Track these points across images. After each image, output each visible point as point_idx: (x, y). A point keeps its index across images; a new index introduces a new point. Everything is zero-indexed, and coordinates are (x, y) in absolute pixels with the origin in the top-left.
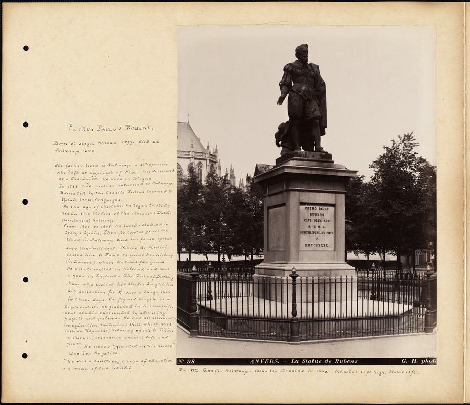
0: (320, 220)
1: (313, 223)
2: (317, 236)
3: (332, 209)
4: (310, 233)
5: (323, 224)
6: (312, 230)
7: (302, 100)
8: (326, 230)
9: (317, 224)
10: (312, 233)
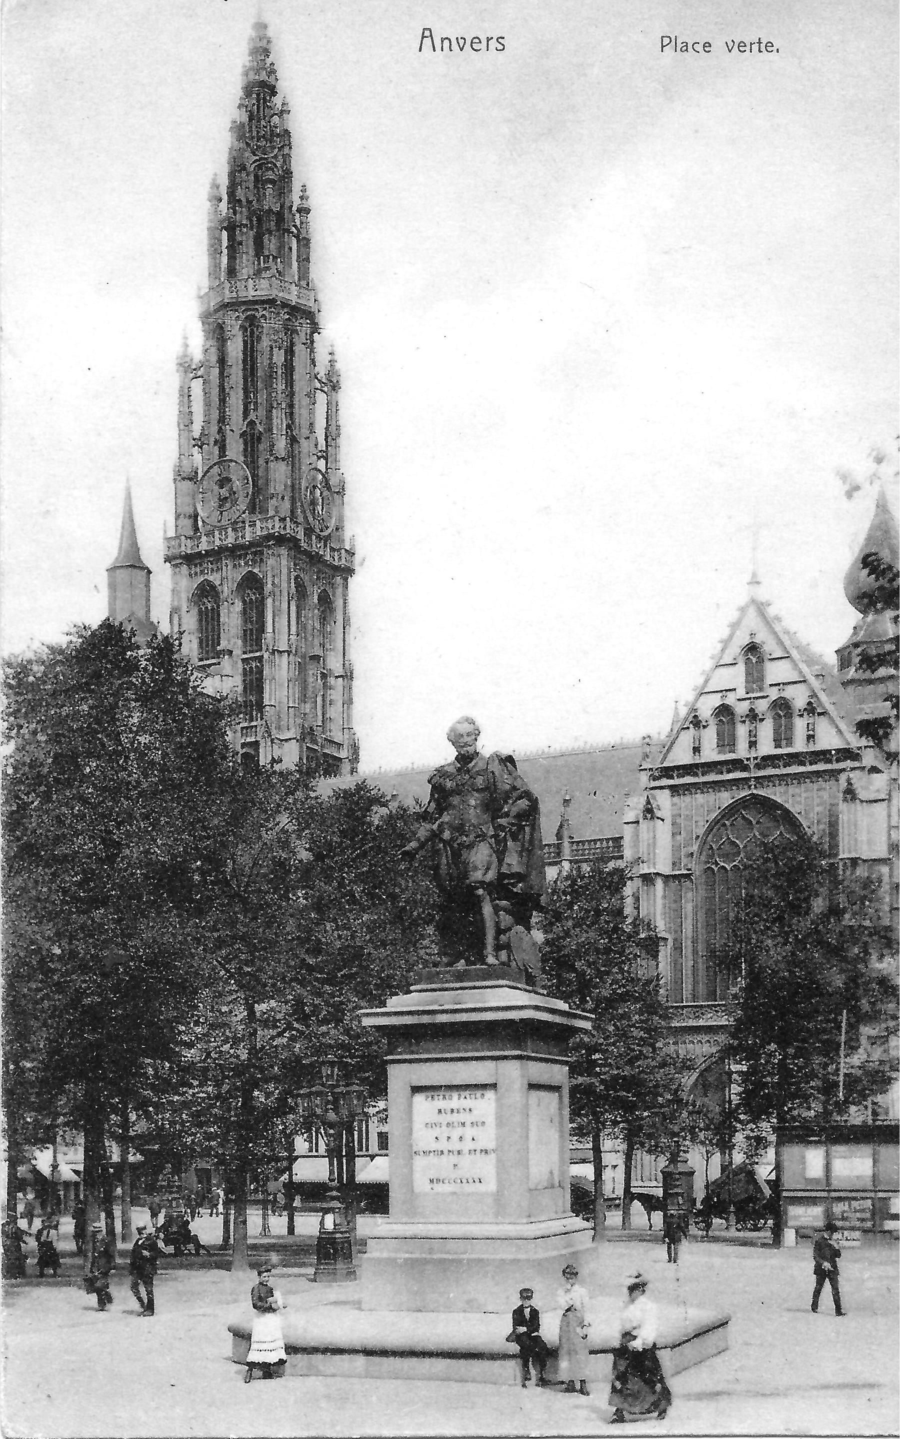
0: (463, 1124)
1: (444, 1132)
2: (454, 1159)
4: (442, 1152)
5: (469, 1132)
6: (443, 1145)
8: (479, 1146)
9: (456, 1133)
10: (446, 1152)
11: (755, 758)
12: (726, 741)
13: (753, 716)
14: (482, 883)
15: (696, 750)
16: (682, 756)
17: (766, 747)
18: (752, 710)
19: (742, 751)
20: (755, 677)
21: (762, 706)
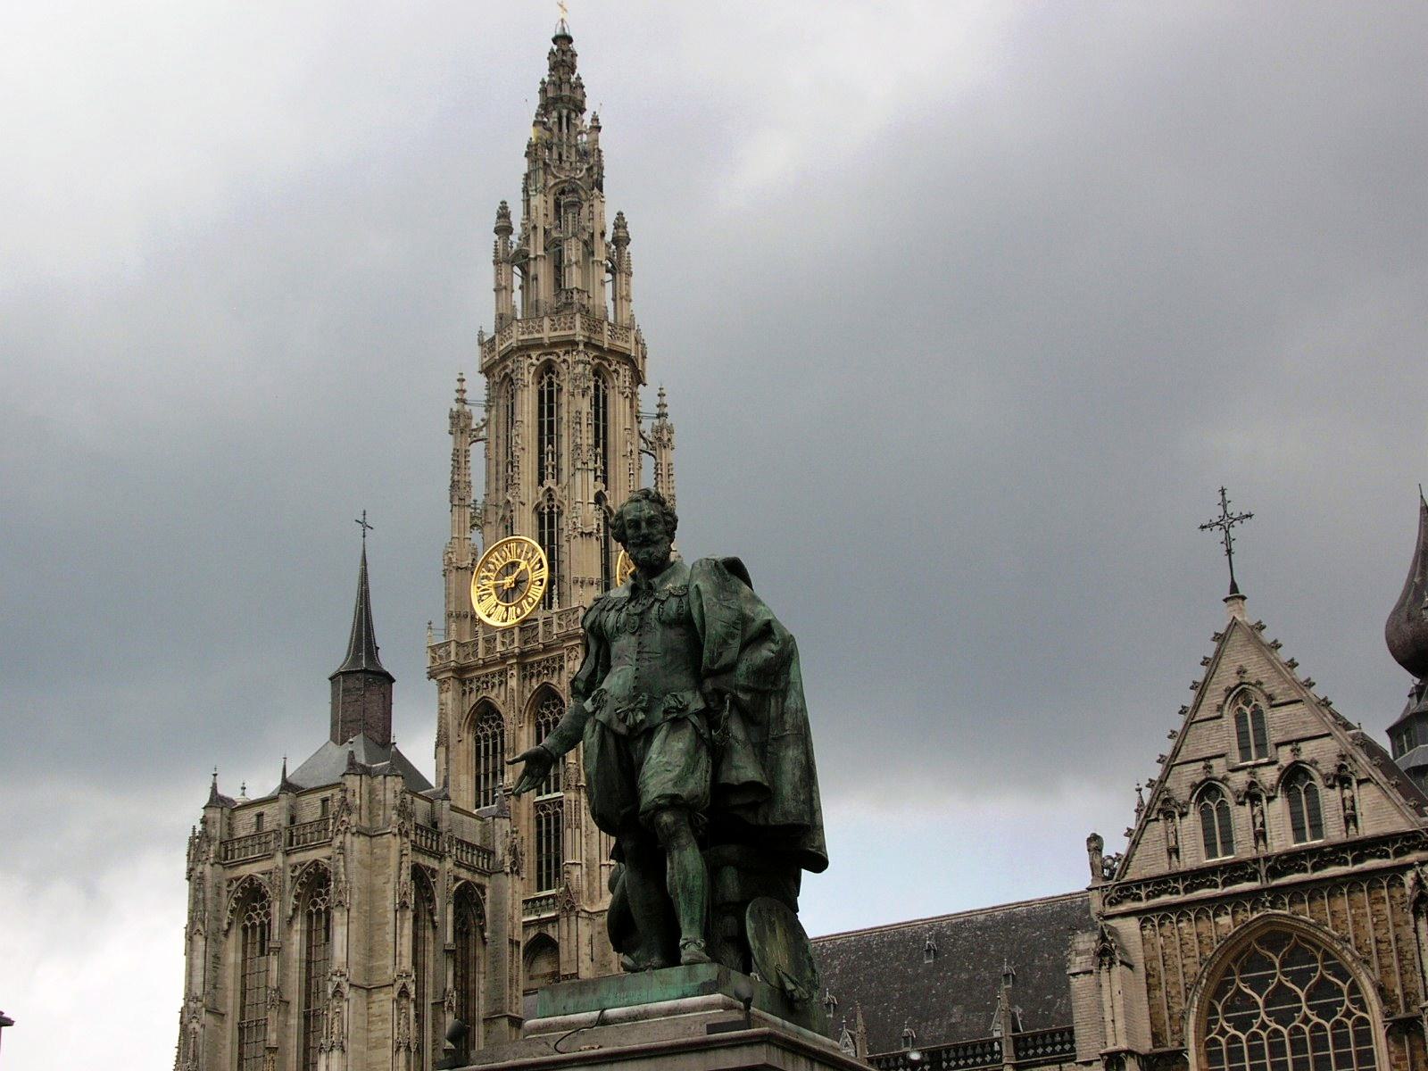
7: (611, 741)
11: (1267, 859)
12: (1217, 833)
13: (1252, 795)
15: (1174, 851)
16: (1152, 863)
17: (1281, 840)
18: (1252, 784)
19: (1244, 848)
20: (1252, 736)
21: (1269, 776)
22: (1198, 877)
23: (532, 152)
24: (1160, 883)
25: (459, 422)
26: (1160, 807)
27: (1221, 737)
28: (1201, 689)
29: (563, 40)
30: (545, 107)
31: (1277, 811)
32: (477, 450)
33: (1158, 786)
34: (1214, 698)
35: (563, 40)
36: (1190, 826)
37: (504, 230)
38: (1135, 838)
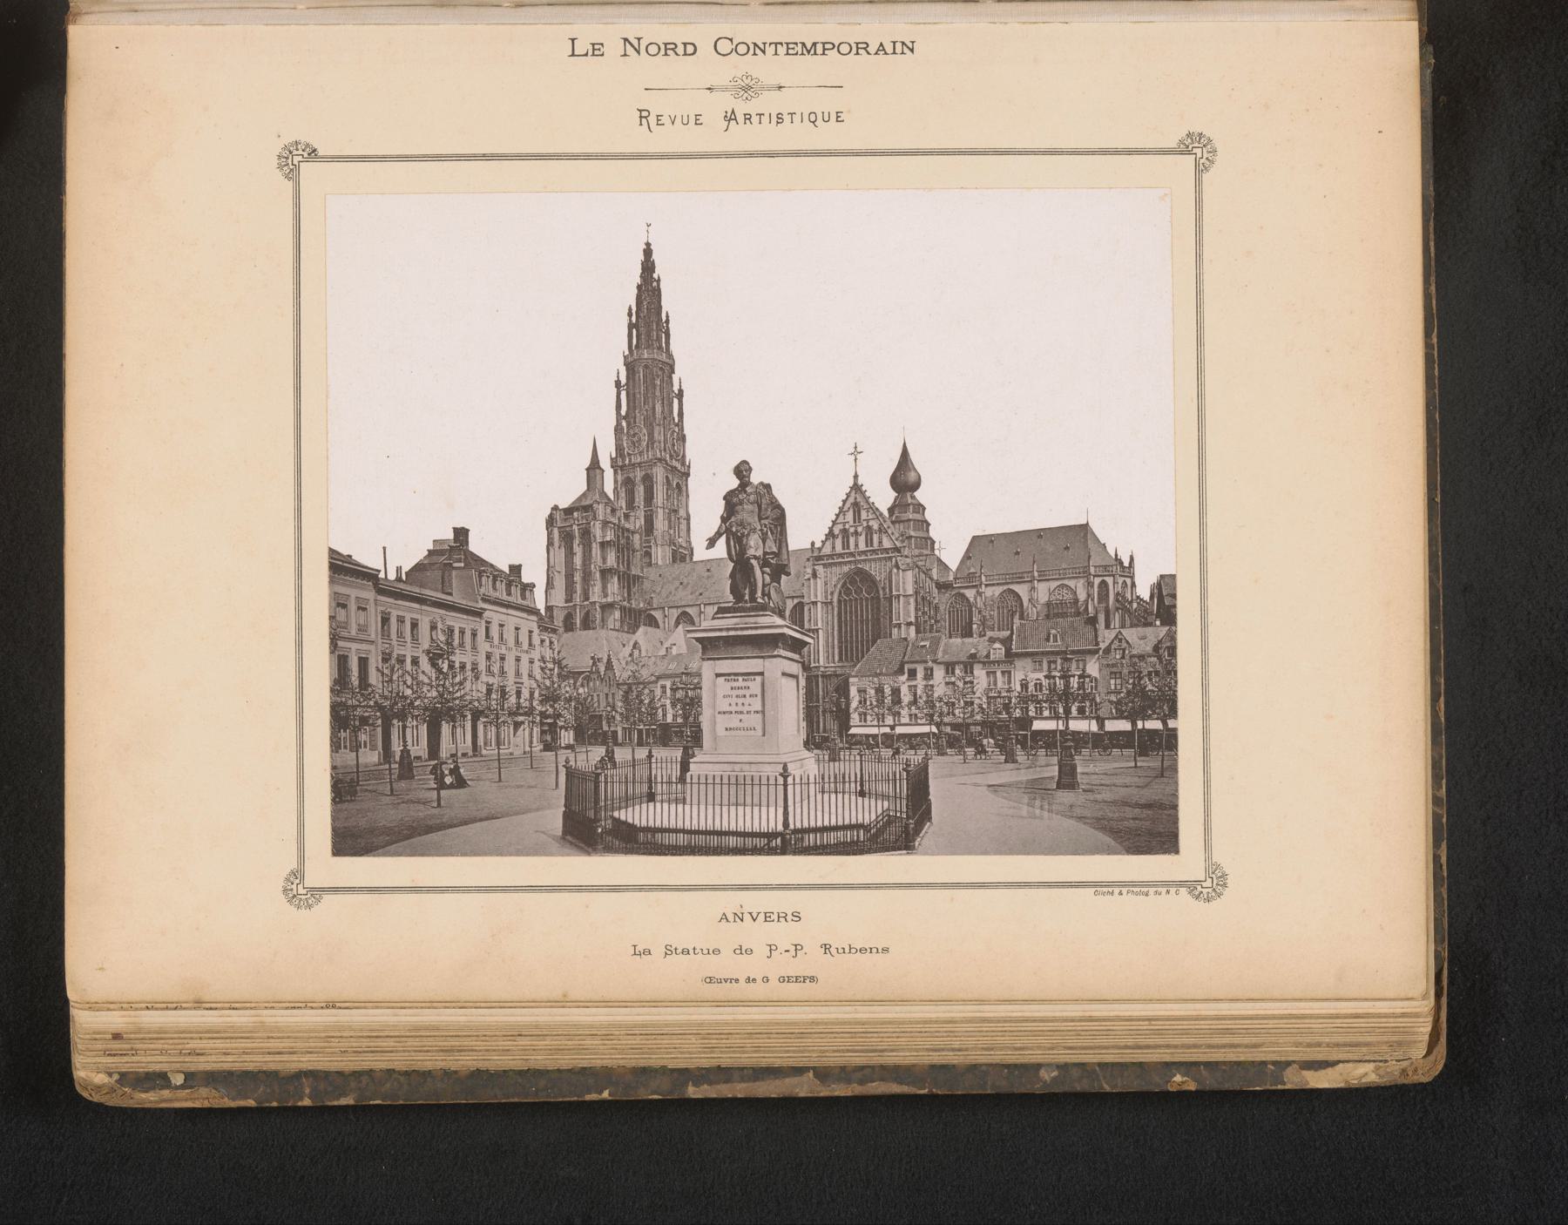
1: (734, 700)
3: (759, 678)
5: (748, 700)
6: (733, 708)
9: (740, 701)
12: (846, 545)
13: (856, 533)
14: (755, 557)
16: (827, 550)
17: (862, 547)
22: (841, 555)
23: (639, 287)
24: (831, 556)
25: (618, 384)
26: (831, 534)
27: (850, 516)
28: (844, 502)
29: (648, 244)
30: (643, 269)
31: (862, 539)
32: (623, 394)
33: (831, 529)
34: (848, 505)
35: (648, 244)
36: (839, 542)
37: (630, 315)
38: (823, 543)
